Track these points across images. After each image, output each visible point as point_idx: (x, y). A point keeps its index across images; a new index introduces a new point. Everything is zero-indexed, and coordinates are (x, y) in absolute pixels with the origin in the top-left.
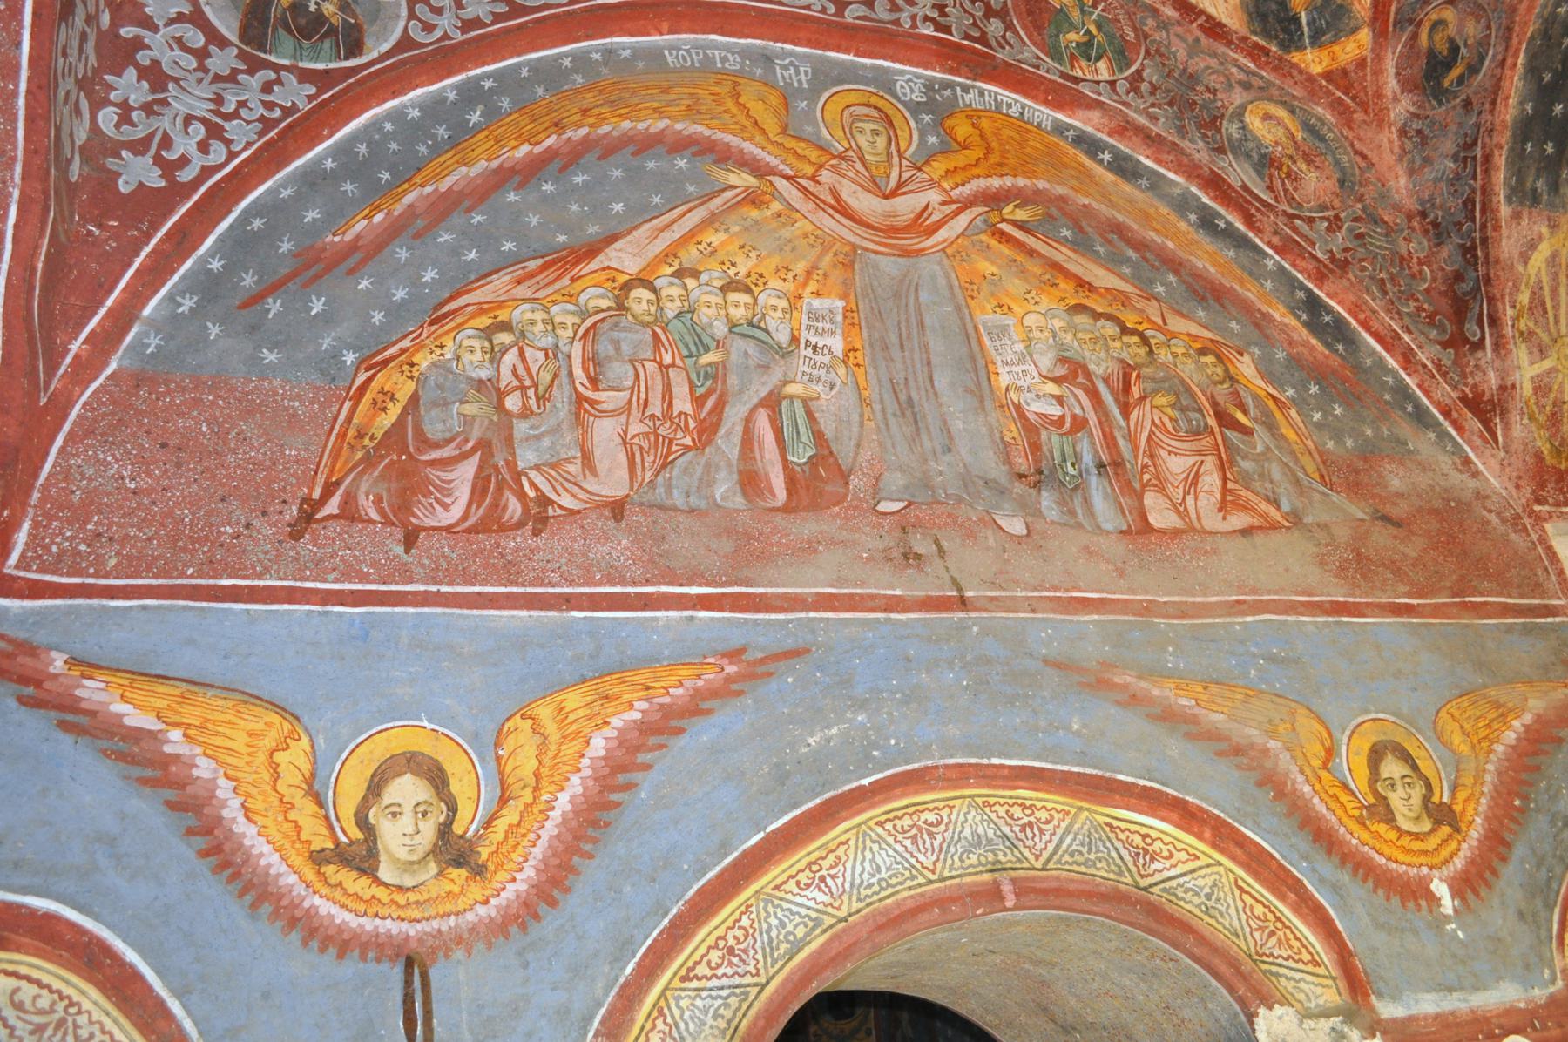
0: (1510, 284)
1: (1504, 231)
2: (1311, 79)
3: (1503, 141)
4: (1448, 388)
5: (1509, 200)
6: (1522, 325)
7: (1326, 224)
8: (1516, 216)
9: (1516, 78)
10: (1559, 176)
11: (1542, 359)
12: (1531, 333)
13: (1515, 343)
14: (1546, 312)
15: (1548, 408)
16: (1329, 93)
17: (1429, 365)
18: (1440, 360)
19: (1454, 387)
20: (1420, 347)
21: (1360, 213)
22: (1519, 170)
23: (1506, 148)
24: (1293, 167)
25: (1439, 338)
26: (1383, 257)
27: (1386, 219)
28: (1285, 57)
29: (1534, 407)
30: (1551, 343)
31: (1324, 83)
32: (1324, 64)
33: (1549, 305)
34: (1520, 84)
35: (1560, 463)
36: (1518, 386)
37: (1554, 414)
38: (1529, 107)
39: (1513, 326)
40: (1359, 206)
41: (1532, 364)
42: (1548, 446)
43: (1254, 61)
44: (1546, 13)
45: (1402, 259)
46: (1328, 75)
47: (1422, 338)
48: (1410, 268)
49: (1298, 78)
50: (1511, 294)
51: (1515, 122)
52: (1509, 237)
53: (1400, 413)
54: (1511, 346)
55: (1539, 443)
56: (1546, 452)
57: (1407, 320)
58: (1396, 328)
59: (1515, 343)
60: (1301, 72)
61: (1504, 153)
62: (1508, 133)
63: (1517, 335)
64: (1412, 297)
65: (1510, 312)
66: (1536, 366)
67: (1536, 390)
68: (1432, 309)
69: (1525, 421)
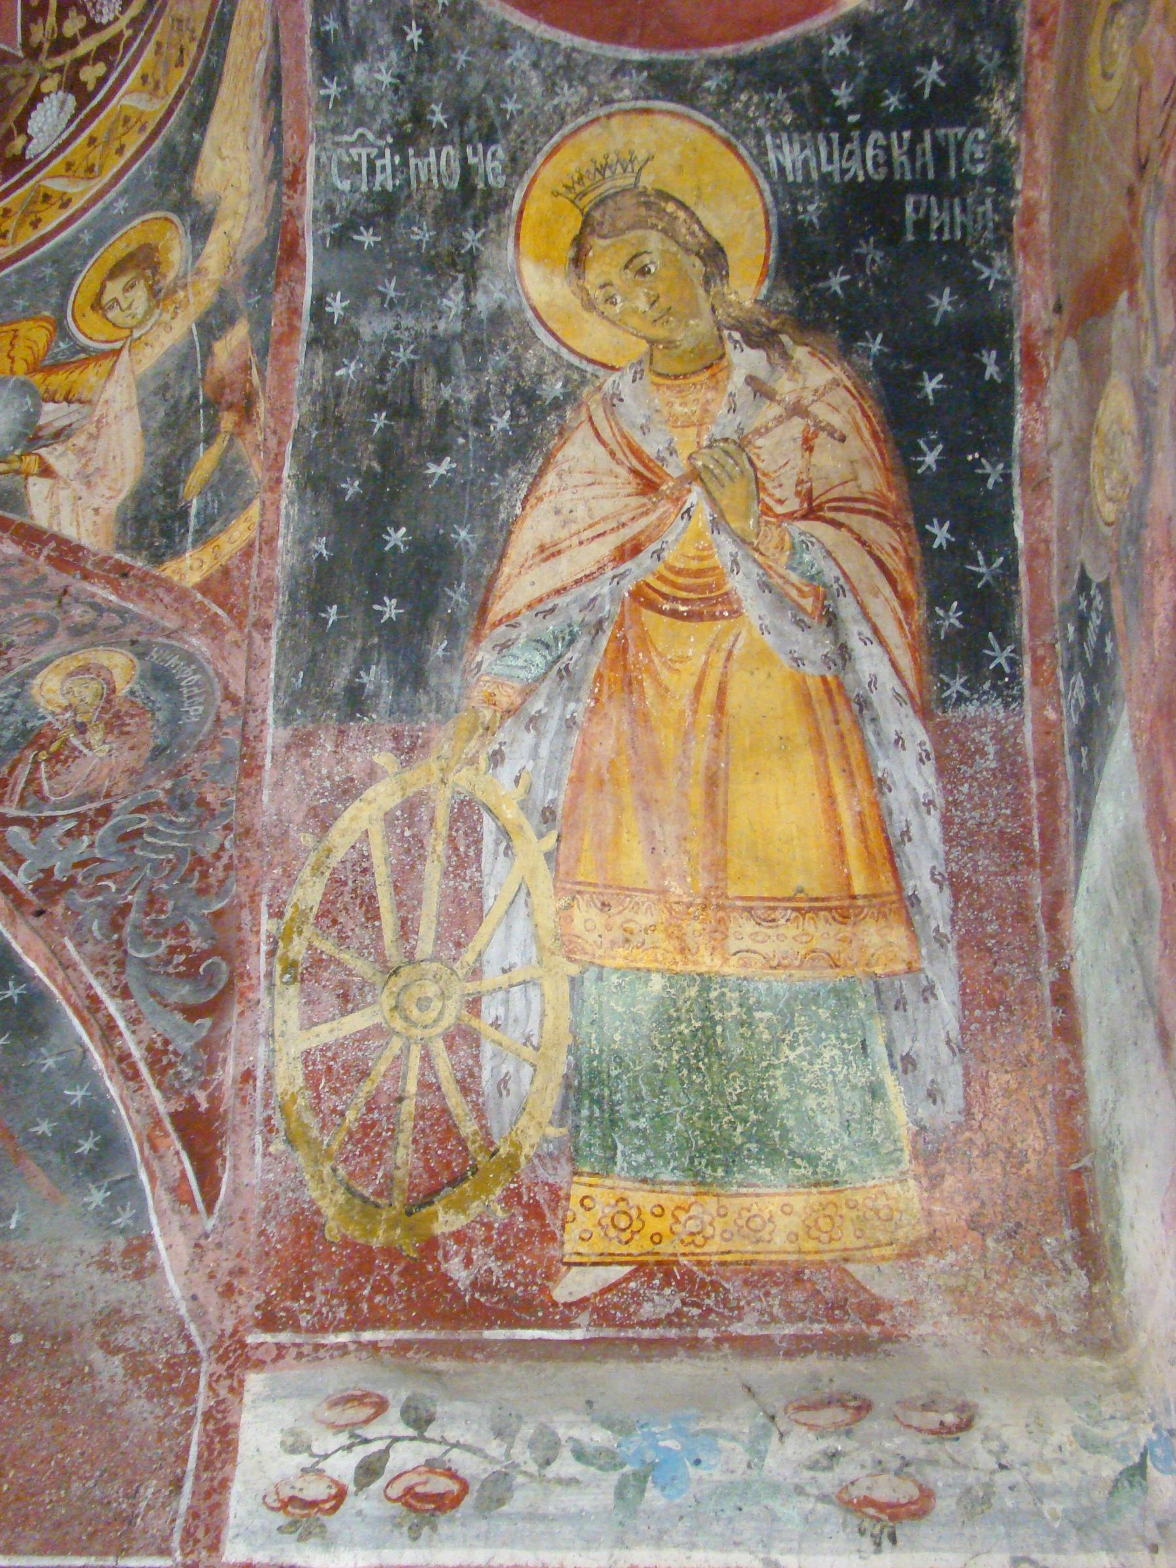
0: (278, 871)
1: (269, 773)
2: (183, 596)
3: (269, 614)
4: (157, 1095)
5: (286, 715)
6: (298, 949)
7: (71, 824)
8: (302, 742)
9: (284, 502)
10: (422, 657)
11: (344, 1013)
12: (318, 962)
13: (271, 987)
14: (373, 914)
15: (351, 1115)
16: (204, 609)
17: (137, 1053)
18: (166, 1042)
19: (168, 1092)
20: (133, 1022)
21: (161, 795)
22: (314, 658)
23: (277, 624)
24: (75, 742)
25: (191, 1001)
26: (157, 868)
27: (210, 798)
28: (156, 572)
29: (309, 1118)
30: (379, 979)
31: (199, 596)
32: (205, 567)
33: (385, 901)
34: (294, 511)
35: (372, 1233)
36: (260, 1074)
37: (366, 1127)
38: (320, 546)
39: (271, 954)
40: (168, 784)
41: (309, 1024)
42: (340, 1197)
43: (116, 590)
44: (316, 385)
45: (200, 861)
46: (204, 587)
47: (147, 1005)
48: (204, 875)
49: (167, 599)
50: (275, 890)
51: (292, 575)
52: (278, 784)
53: (55, 1158)
54: (262, 994)
55: (313, 1192)
56: (329, 1211)
57: (132, 975)
58: (100, 991)
59: (271, 987)
60: (170, 590)
61: (274, 634)
62: (282, 598)
63: (278, 969)
64: (180, 930)
65: (267, 925)
66: (324, 1029)
67: (312, 1080)
68: (205, 946)
69: (278, 1146)
